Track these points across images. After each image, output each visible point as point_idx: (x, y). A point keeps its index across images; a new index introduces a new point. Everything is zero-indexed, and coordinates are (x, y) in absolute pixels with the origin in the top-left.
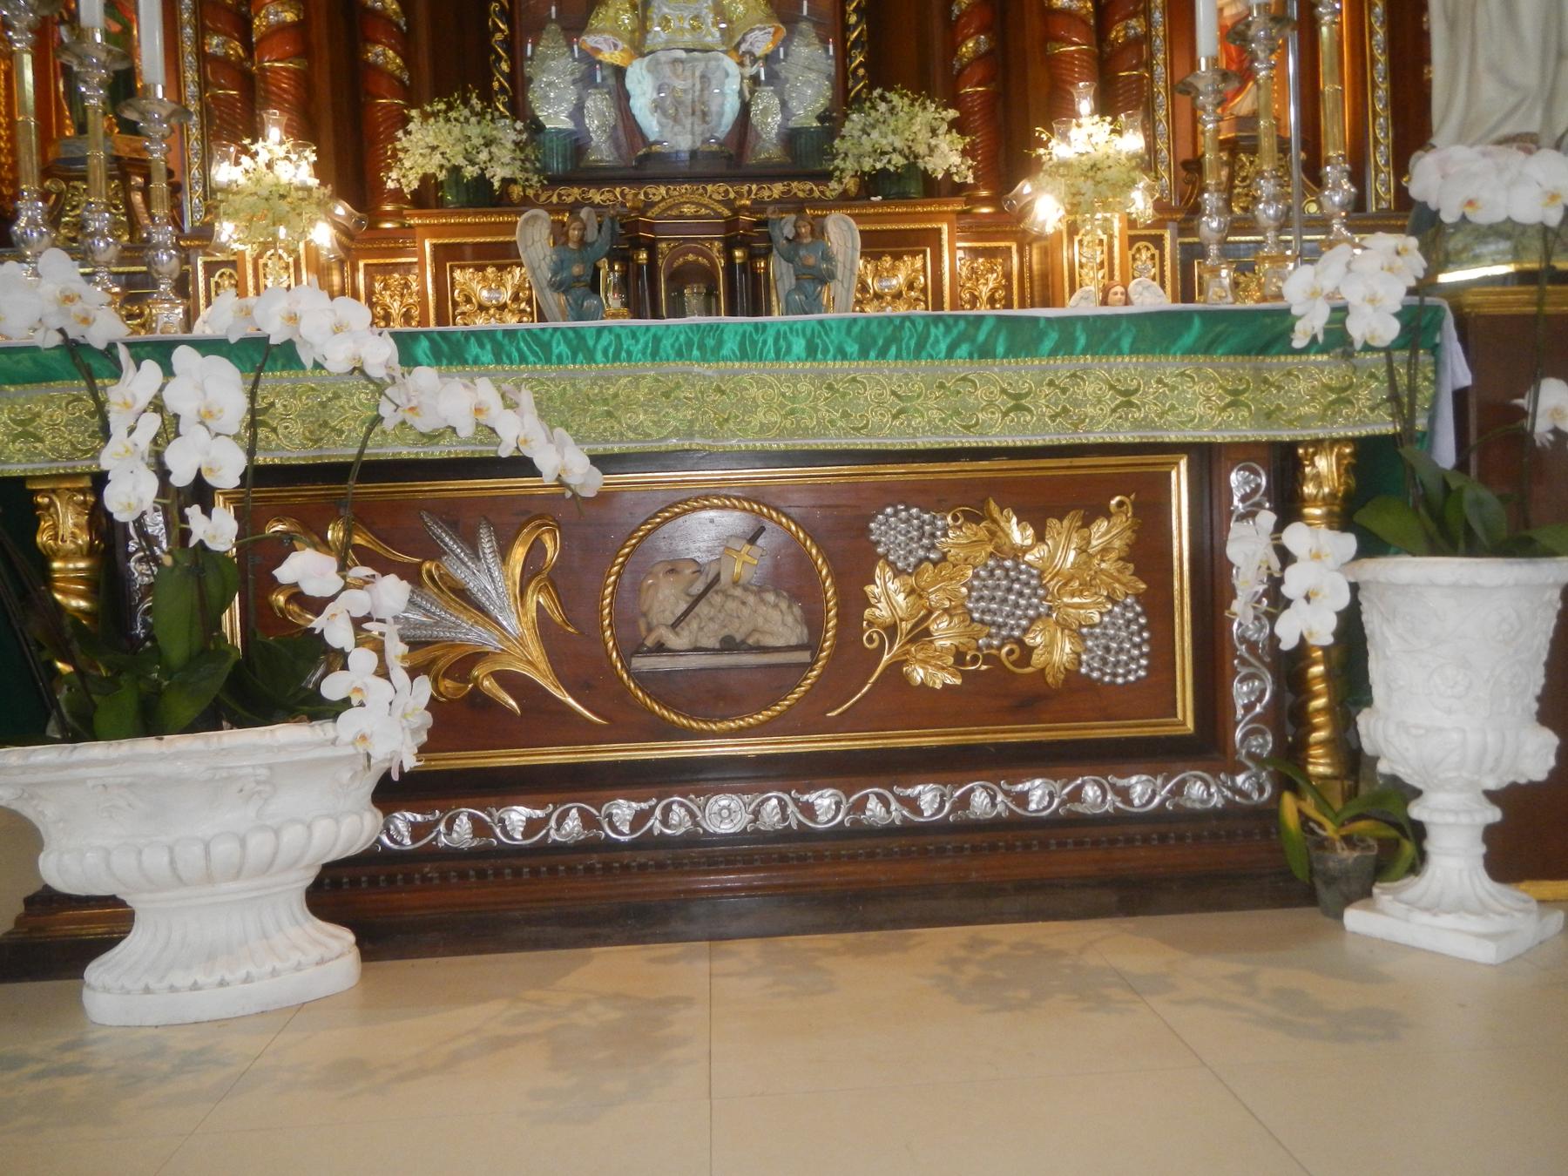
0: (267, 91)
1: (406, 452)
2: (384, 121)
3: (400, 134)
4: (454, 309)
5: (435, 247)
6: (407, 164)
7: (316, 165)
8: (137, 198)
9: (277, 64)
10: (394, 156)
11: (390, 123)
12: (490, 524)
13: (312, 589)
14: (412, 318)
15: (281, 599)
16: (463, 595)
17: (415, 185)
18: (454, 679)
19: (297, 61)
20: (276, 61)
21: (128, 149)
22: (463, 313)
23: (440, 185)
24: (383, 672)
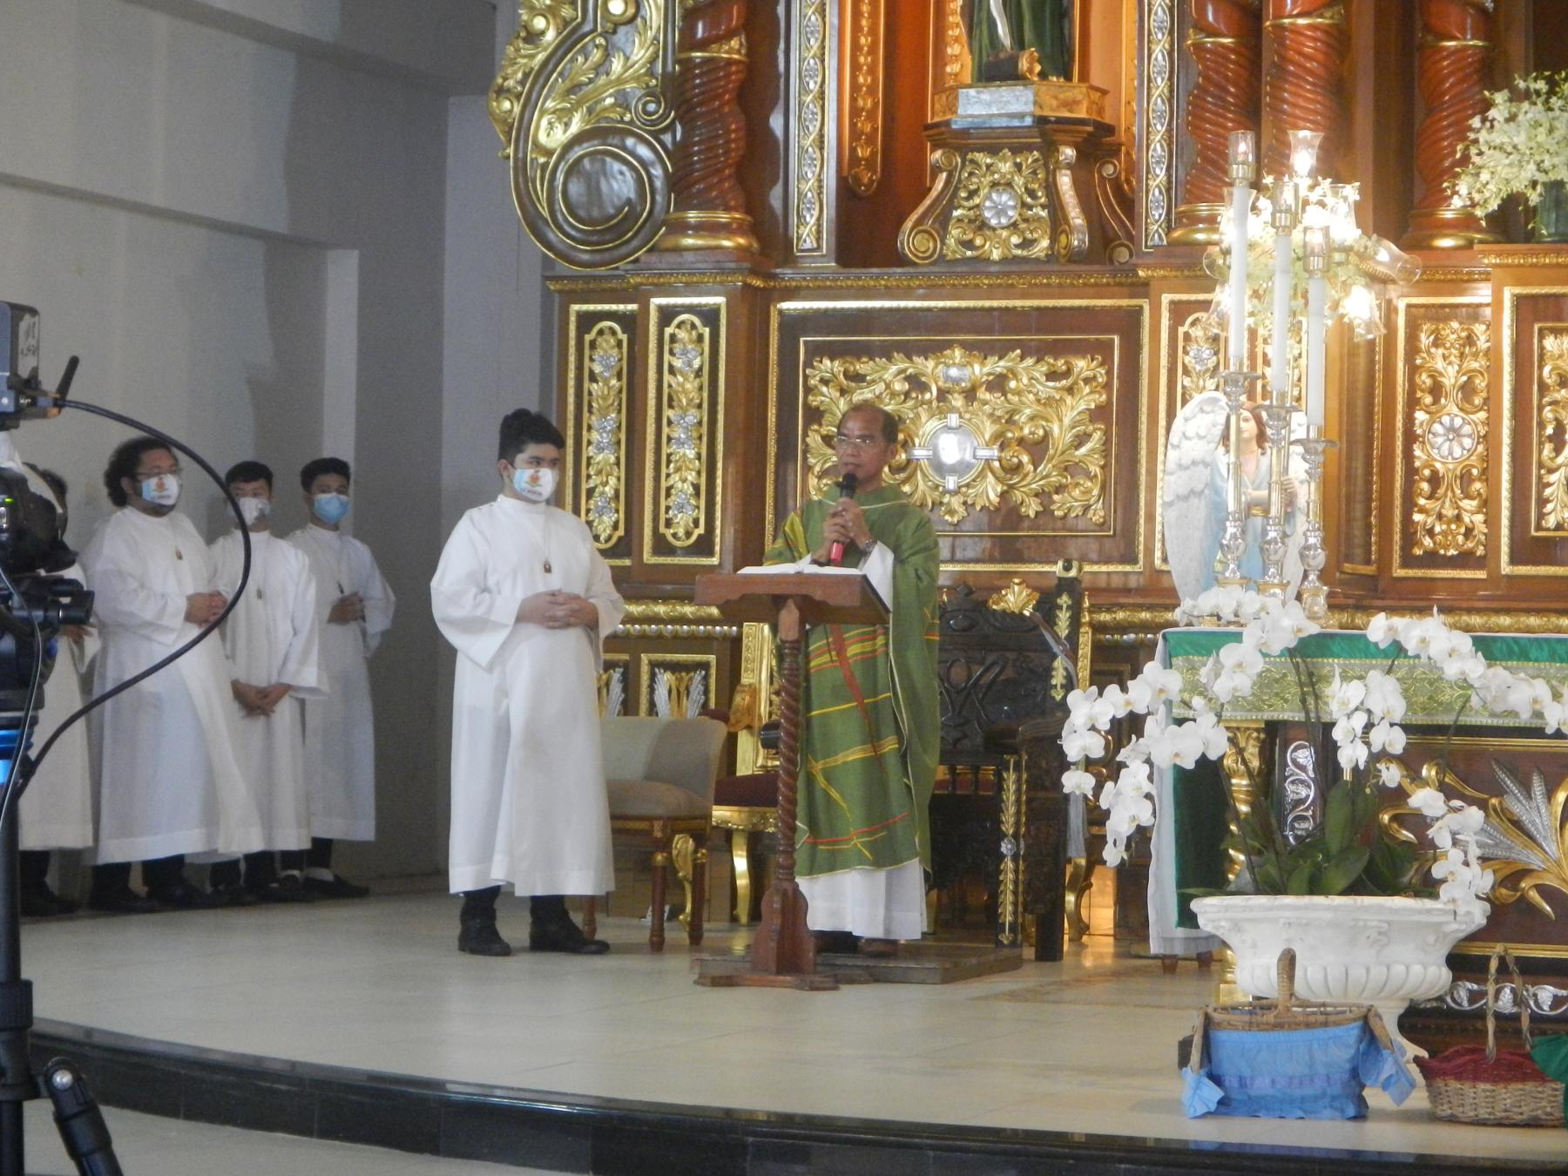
0: (1282, 57)
1: (1485, 720)
2: (1451, 74)
3: (1476, 122)
4: (1541, 396)
5: (1520, 301)
6: (1485, 176)
7: (1358, 207)
8: (1065, 181)
9: (1301, 21)
10: (1465, 160)
11: (1461, 74)
12: (1541, 773)
13: (1426, 812)
14: (1474, 391)
15: (1386, 818)
16: (1517, 824)
17: (1494, 205)
18: (1508, 889)
19: (1328, 14)
20: (1299, 15)
21: (1055, 103)
22: (1554, 403)
23: (1532, 212)
24: (1466, 864)
